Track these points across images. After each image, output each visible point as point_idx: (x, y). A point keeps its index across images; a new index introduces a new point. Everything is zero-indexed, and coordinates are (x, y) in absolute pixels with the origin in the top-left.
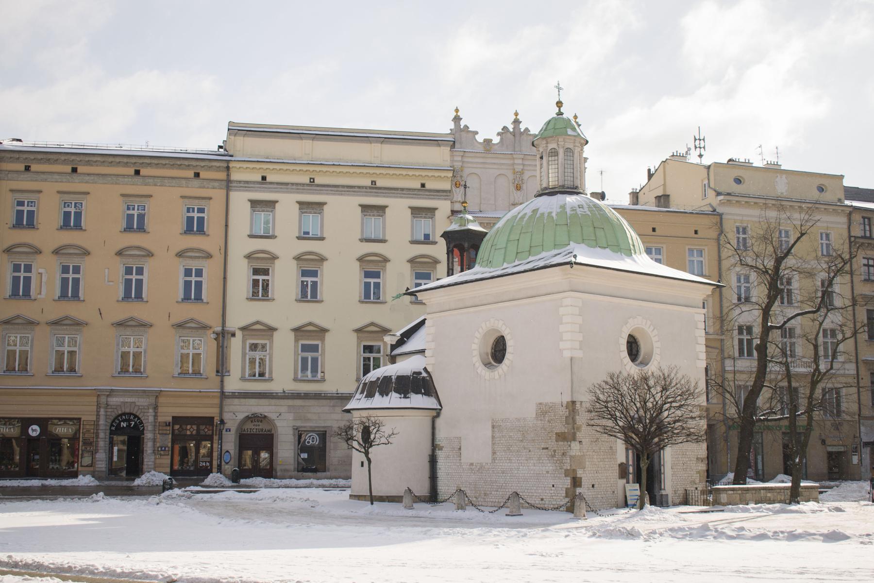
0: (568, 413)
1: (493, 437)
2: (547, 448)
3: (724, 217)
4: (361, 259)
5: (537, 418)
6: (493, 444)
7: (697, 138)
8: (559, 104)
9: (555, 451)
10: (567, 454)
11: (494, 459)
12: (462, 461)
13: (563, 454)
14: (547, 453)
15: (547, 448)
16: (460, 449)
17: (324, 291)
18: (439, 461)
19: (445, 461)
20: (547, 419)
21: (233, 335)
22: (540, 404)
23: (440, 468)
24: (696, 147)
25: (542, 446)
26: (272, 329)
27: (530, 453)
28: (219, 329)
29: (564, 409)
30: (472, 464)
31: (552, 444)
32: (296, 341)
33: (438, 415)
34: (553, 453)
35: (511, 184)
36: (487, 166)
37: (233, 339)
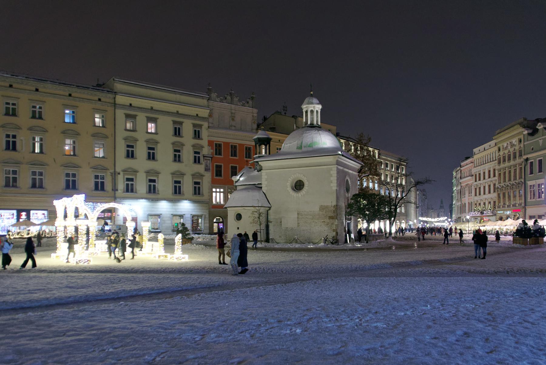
1: (298, 218)
2: (324, 222)
4: (173, 144)
5: (320, 210)
9: (328, 223)
11: (298, 226)
13: (332, 224)
15: (324, 222)
16: (281, 222)
17: (158, 156)
20: (324, 211)
21: (119, 174)
26: (136, 172)
28: (112, 171)
29: (332, 208)
30: (287, 228)
31: (327, 220)
32: (147, 177)
33: (270, 209)
37: (119, 175)
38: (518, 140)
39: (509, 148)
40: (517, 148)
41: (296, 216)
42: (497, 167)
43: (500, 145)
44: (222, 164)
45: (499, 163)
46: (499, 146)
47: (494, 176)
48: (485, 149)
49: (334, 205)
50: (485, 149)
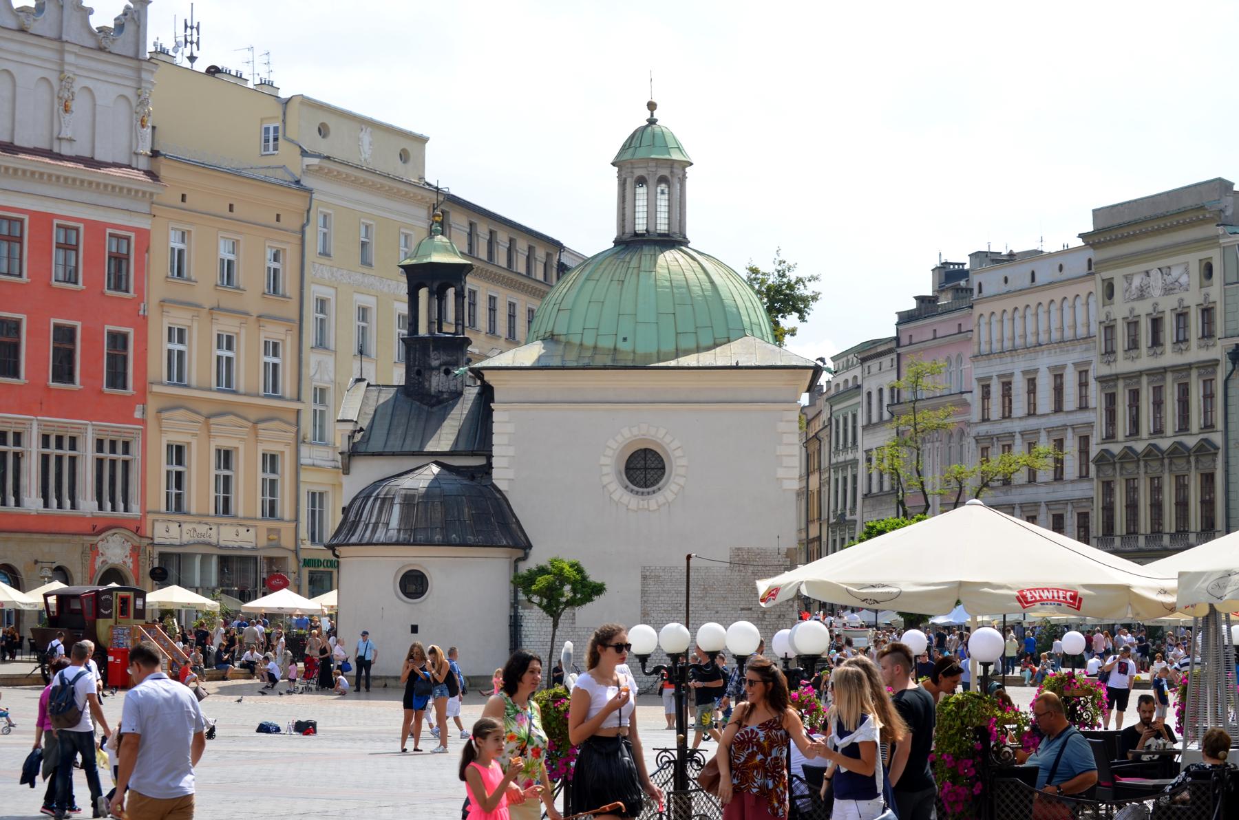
0: (788, 563)
1: (643, 592)
2: (751, 609)
3: (314, 196)
6: (644, 602)
7: (189, 24)
8: (652, 106)
10: (787, 616)
12: (577, 625)
13: (779, 616)
14: (750, 616)
15: (751, 609)
18: (524, 624)
19: (539, 624)
22: (738, 549)
23: (526, 636)
24: (186, 41)
25: (742, 606)
27: (718, 615)
34: (761, 616)
35: (56, 100)
36: (26, 60)
38: (1195, 269)
39: (1156, 292)
40: (1193, 299)
41: (637, 585)
42: (1099, 369)
43: (1117, 275)
44: (24, 317)
45: (1109, 352)
46: (1106, 275)
47: (1083, 407)
48: (1033, 280)
49: (789, 549)
50: (1033, 280)
